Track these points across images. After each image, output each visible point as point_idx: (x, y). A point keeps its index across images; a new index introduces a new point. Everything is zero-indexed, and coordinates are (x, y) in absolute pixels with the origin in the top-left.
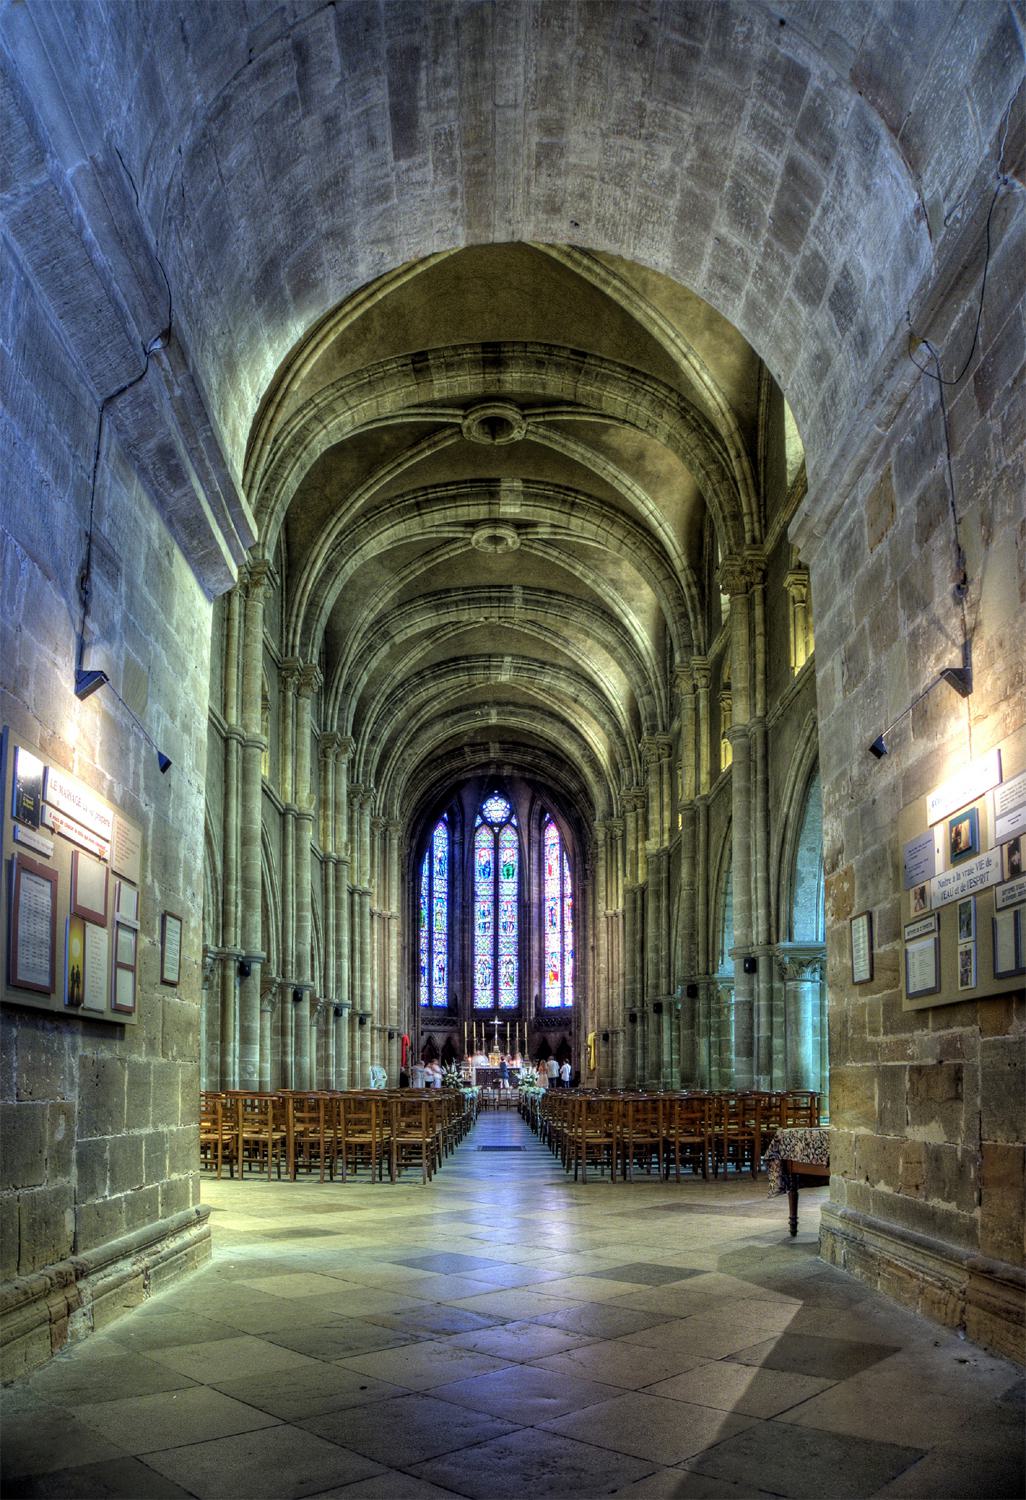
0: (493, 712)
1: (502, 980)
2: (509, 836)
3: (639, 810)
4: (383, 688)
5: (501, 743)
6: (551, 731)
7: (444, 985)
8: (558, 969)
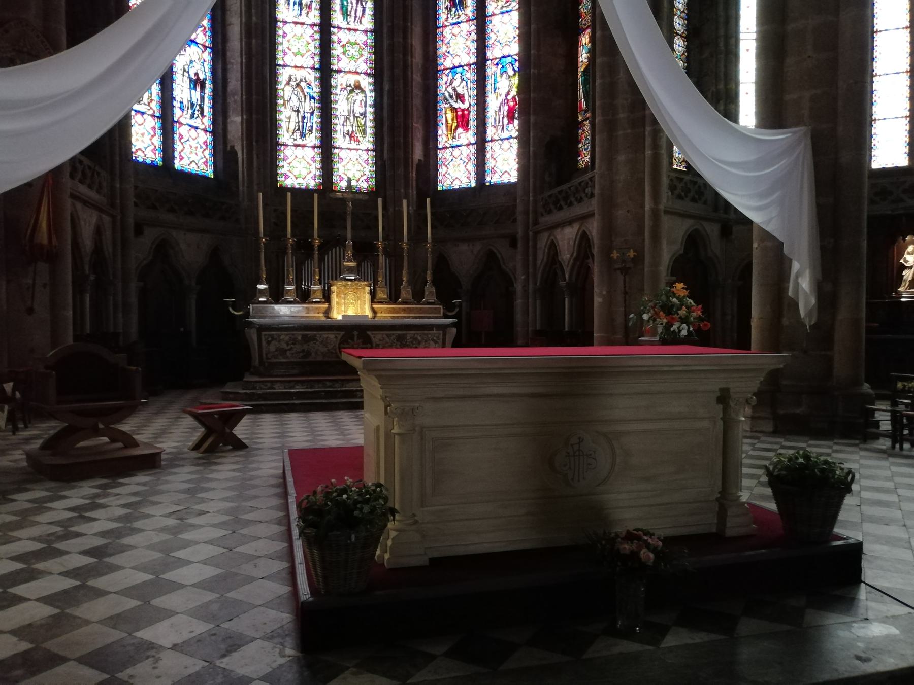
7: (207, 122)
8: (470, 102)
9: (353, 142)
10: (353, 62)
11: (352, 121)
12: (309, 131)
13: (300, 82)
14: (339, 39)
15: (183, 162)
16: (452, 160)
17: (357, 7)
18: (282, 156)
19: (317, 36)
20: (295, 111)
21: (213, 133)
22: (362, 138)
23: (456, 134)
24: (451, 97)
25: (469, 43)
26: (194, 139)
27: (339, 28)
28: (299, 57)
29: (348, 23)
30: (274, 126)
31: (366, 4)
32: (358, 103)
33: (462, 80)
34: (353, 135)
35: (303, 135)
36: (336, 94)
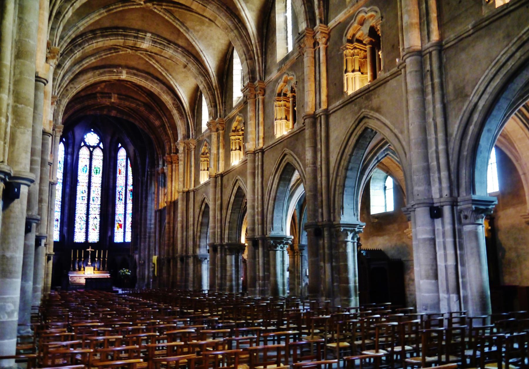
0: (124, 72)
1: (91, 227)
2: (98, 154)
3: (221, 132)
4: (70, 33)
5: (118, 94)
6: (155, 88)
8: (122, 222)
30: (74, 227)
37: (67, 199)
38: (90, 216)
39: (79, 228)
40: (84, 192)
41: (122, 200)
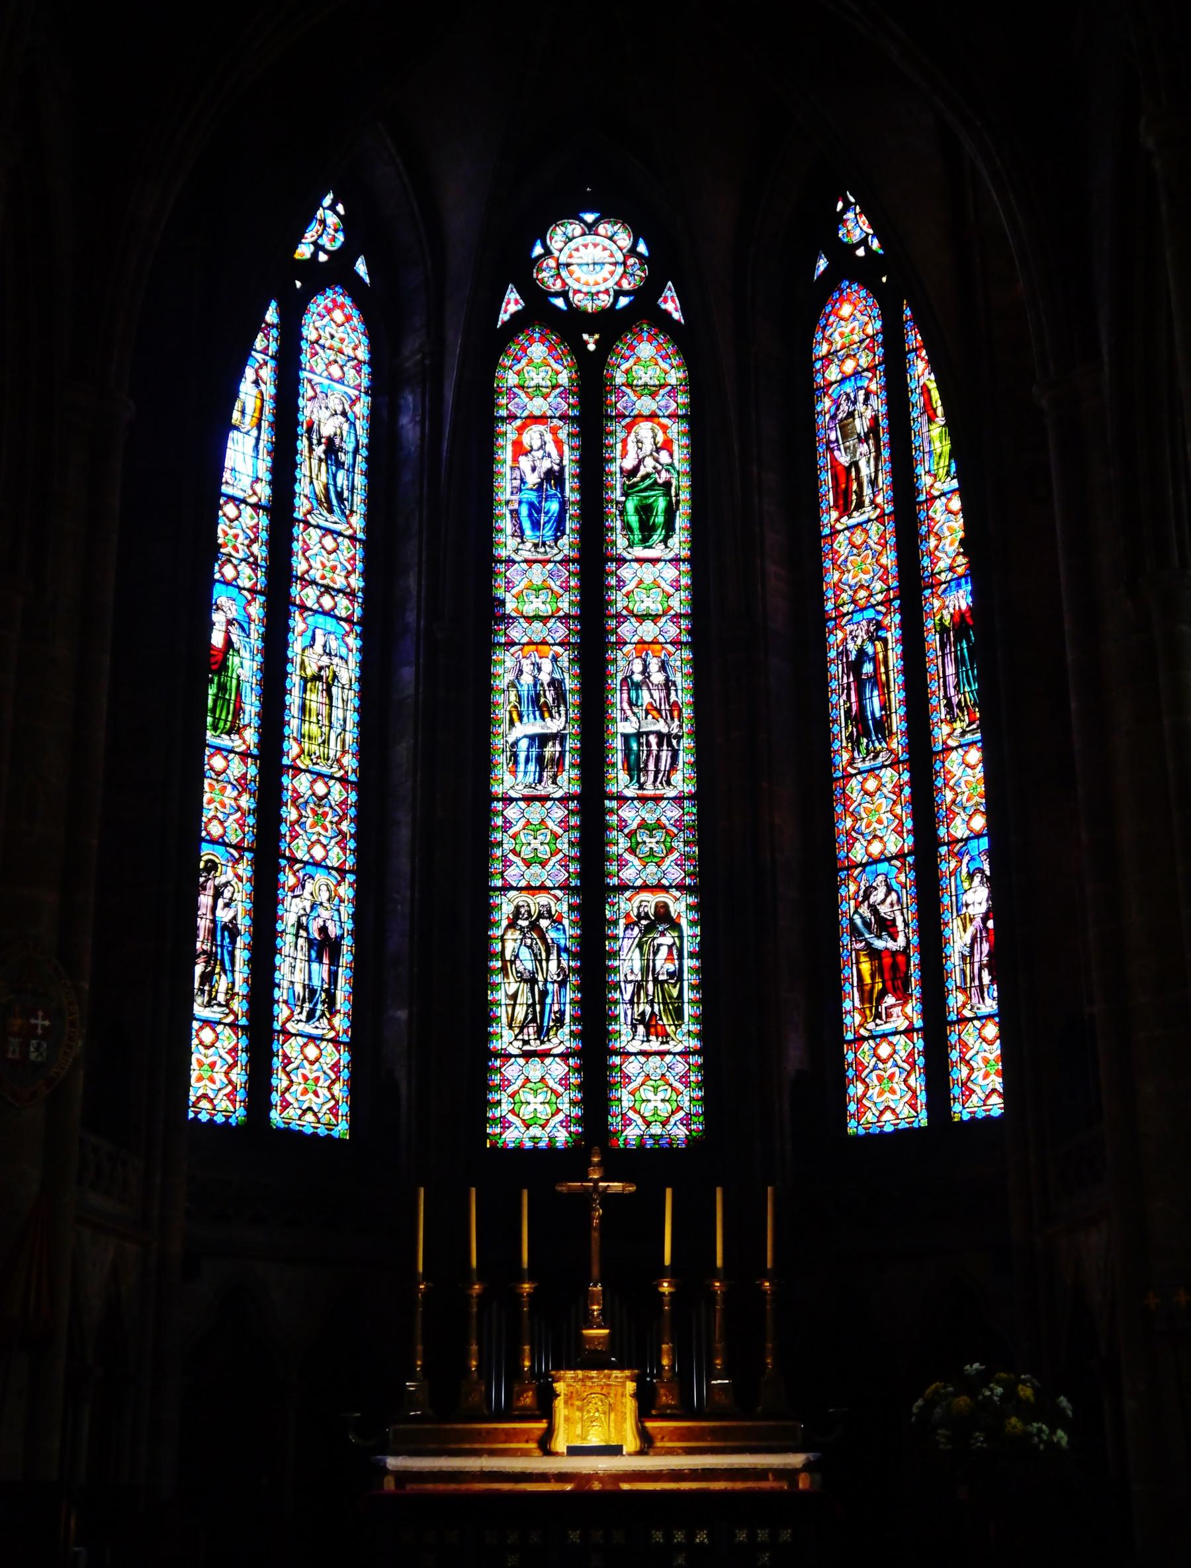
7: (341, 1022)
9: (653, 1038)
10: (652, 868)
11: (651, 992)
12: (556, 1020)
13: (537, 919)
14: (621, 820)
15: (292, 1112)
16: (875, 1068)
17: (659, 751)
18: (497, 1079)
19: (574, 820)
20: (526, 981)
21: (352, 1046)
22: (673, 1028)
23: (882, 1009)
24: (867, 924)
25: (898, 809)
26: (312, 1063)
27: (622, 799)
28: (536, 869)
29: (641, 787)
30: (483, 1016)
31: (678, 743)
32: (664, 951)
33: (890, 890)
34: (654, 1023)
35: (542, 1033)
36: (616, 938)
37: (403, 751)
38: (626, 905)
39: (520, 1012)
40: (550, 696)
41: (882, 728)
